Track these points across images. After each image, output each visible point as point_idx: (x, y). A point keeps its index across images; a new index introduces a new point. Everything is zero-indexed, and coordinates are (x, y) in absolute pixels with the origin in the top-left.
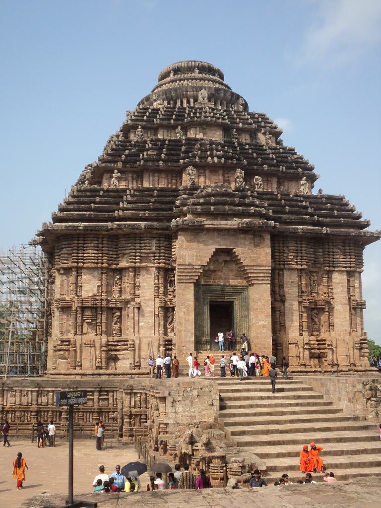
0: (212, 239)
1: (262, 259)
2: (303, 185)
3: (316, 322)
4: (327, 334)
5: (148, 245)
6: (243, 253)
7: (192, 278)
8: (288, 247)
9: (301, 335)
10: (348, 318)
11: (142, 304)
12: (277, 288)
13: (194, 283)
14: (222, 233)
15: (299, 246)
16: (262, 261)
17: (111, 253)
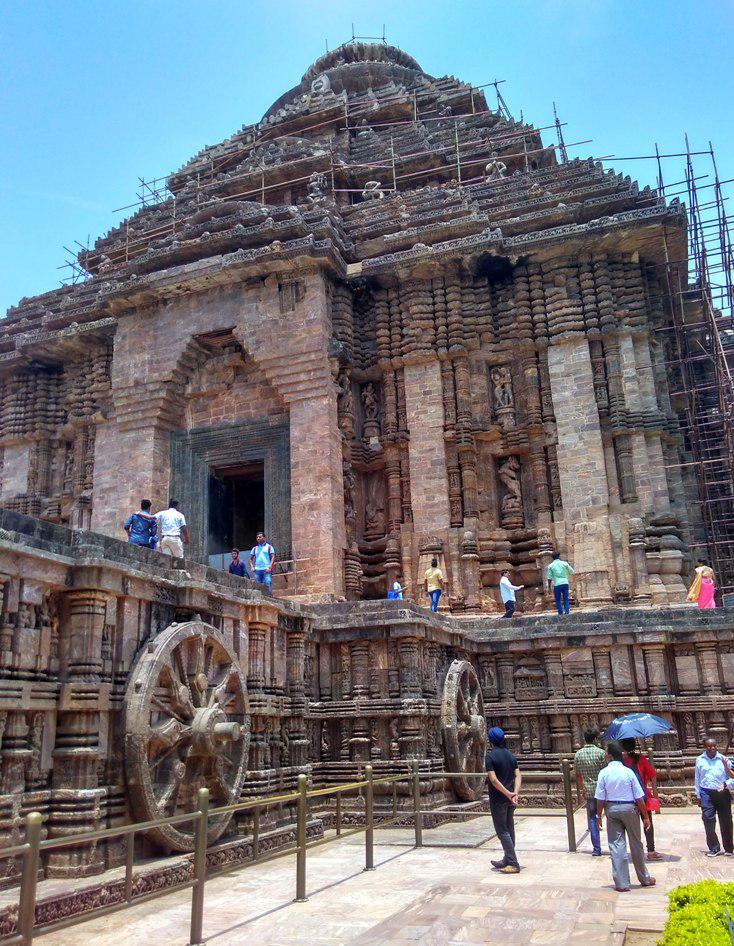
0: (184, 317)
1: (299, 338)
2: (489, 173)
3: (510, 491)
4: (544, 516)
5: (101, 371)
6: (253, 334)
7: (148, 414)
8: (407, 310)
9: (457, 525)
10: (600, 465)
11: (96, 501)
12: (391, 418)
13: (156, 427)
14: (208, 298)
15: (442, 299)
16: (298, 343)
17: (53, 407)
